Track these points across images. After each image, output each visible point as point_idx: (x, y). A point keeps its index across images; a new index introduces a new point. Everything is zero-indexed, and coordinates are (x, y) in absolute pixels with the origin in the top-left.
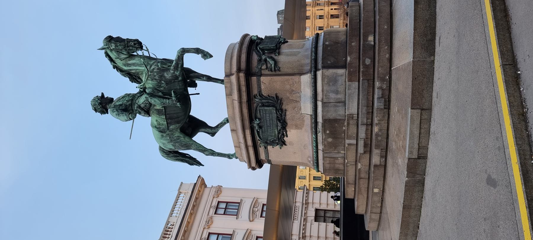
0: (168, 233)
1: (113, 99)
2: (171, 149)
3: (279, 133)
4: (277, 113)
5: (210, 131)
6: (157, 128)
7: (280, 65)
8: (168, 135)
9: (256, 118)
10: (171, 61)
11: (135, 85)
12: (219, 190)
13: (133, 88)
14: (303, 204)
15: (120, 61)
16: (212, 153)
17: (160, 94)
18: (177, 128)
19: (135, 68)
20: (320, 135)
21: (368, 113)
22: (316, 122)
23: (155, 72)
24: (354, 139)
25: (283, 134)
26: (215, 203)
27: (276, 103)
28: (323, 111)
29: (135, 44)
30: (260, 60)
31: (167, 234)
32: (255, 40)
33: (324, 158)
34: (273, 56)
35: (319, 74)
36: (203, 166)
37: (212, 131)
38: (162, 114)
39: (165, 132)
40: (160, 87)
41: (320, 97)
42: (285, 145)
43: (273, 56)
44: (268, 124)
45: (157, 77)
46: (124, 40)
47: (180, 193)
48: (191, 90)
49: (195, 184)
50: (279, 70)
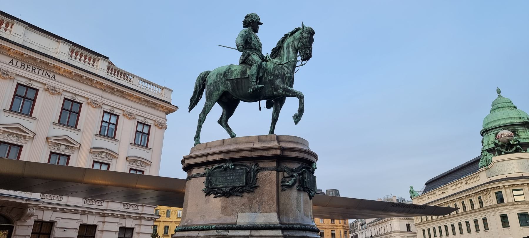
0: (122, 76)
1: (257, 32)
2: (208, 82)
3: (219, 189)
5: (224, 119)
6: (228, 70)
7: (288, 191)
9: (235, 165)
10: (291, 86)
11: (270, 53)
12: (162, 126)
13: (266, 51)
14: (140, 214)
15: (292, 40)
16: (201, 121)
17: (261, 74)
18: (227, 88)
19: (285, 53)
20: (214, 233)
22: (228, 229)
23: (281, 72)
25: (217, 193)
26: (149, 122)
27: (250, 186)
28: (240, 236)
29: (307, 54)
30: (292, 170)
31: (121, 75)
32: (312, 166)
34: (297, 184)
35: (278, 233)
37: (223, 122)
38: (241, 75)
39: (224, 77)
40: (268, 74)
41: (255, 233)
42: (206, 196)
43: (297, 184)
44: (228, 178)
45: (276, 72)
46: (311, 45)
47: (162, 88)
48: (264, 102)
49: (170, 104)
50: (282, 190)
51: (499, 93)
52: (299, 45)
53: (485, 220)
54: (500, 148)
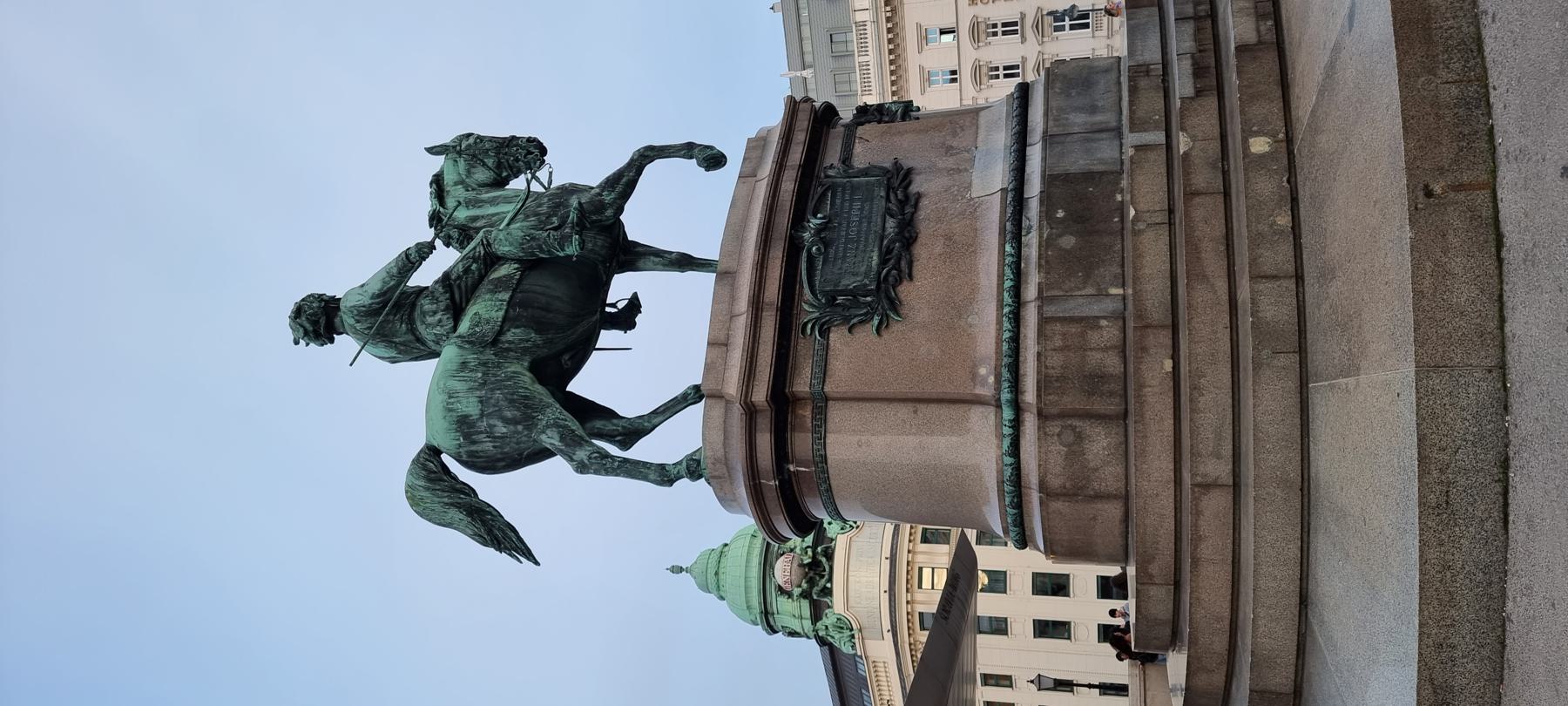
3: (883, 262)
4: (888, 199)
8: (485, 364)
18: (525, 351)
20: (1032, 242)
24: (1157, 128)
25: (897, 267)
33: (1043, 321)
36: (537, 563)
44: (853, 235)
51: (681, 570)
52: (490, 162)
53: (988, 680)
54: (815, 589)
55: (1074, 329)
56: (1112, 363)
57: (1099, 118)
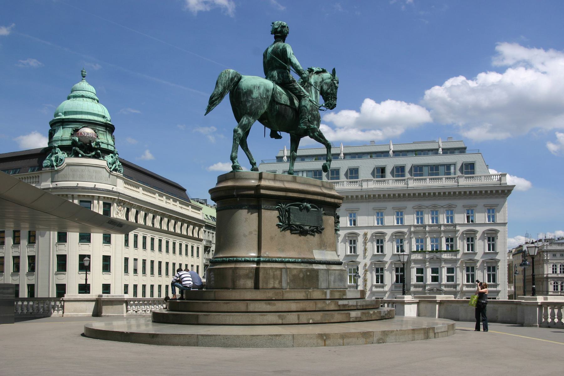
3: (297, 226)
20: (303, 266)
21: (363, 306)
54: (78, 149)
55: (279, 277)
56: (271, 286)
57: (332, 283)
